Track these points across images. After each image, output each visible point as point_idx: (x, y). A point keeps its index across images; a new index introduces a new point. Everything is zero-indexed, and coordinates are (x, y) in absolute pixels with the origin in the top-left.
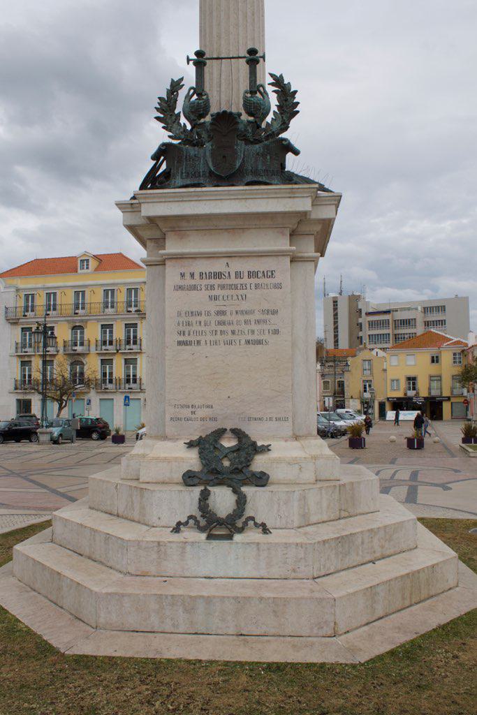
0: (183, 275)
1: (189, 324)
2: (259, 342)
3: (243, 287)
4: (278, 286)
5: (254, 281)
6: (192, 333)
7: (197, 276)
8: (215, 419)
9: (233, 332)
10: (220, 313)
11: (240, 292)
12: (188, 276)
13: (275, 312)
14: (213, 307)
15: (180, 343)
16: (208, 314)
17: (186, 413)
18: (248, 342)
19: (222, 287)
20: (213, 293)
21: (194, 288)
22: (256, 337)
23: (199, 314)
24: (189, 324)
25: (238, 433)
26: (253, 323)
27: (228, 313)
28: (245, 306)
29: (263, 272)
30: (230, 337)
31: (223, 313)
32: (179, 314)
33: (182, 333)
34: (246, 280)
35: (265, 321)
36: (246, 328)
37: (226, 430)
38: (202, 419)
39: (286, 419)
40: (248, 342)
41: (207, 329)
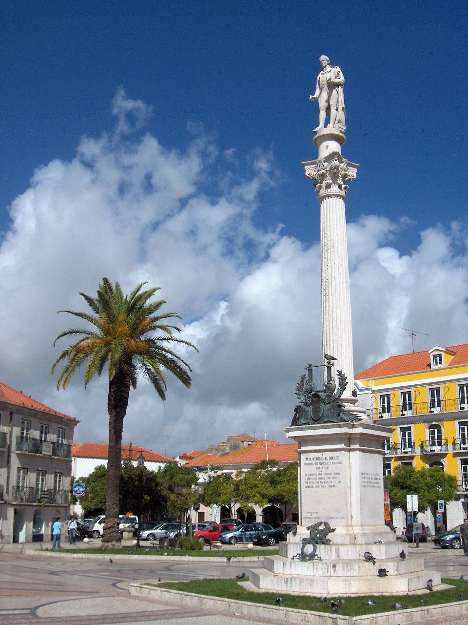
0: (307, 459)
1: (309, 479)
2: (334, 486)
4: (340, 463)
5: (333, 461)
7: (312, 459)
11: (327, 466)
12: (309, 459)
13: (339, 474)
14: (317, 472)
16: (316, 475)
17: (309, 515)
18: (330, 486)
19: (321, 463)
20: (317, 466)
21: (311, 464)
23: (313, 475)
24: (309, 479)
25: (326, 524)
28: (328, 471)
30: (324, 484)
31: (321, 474)
32: (306, 475)
33: (306, 483)
34: (329, 461)
35: (336, 478)
36: (328, 480)
40: (330, 486)
41: (316, 481)
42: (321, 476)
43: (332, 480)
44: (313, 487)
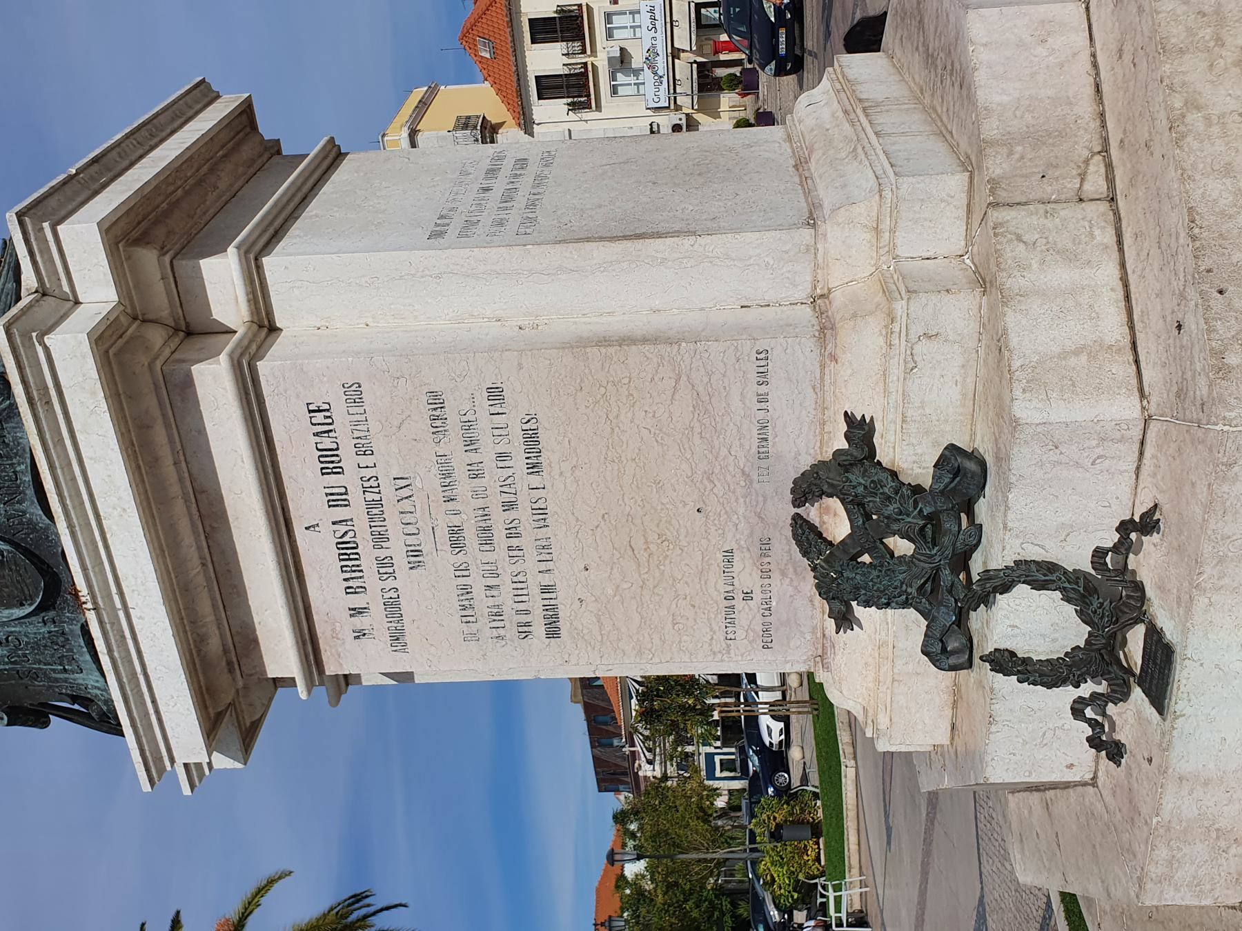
0: (360, 634)
2: (532, 438)
3: (370, 485)
4: (354, 394)
5: (348, 458)
6: (522, 606)
7: (358, 601)
8: (765, 546)
9: (509, 506)
10: (456, 539)
12: (360, 622)
13: (436, 402)
14: (442, 560)
15: (553, 632)
16: (462, 570)
17: (747, 614)
18: (534, 468)
19: (380, 538)
20: (401, 560)
21: (392, 606)
22: (517, 449)
23: (466, 590)
26: (474, 457)
27: (456, 521)
28: (427, 480)
29: (316, 434)
30: (523, 514)
31: (456, 534)
32: (474, 637)
33: (525, 631)
34: (350, 479)
35: (468, 425)
36: (492, 476)
37: (797, 518)
38: (766, 574)
39: (763, 355)
40: (534, 468)
41: (507, 570)
42: (470, 536)
43: (487, 454)
44: (546, 589)
